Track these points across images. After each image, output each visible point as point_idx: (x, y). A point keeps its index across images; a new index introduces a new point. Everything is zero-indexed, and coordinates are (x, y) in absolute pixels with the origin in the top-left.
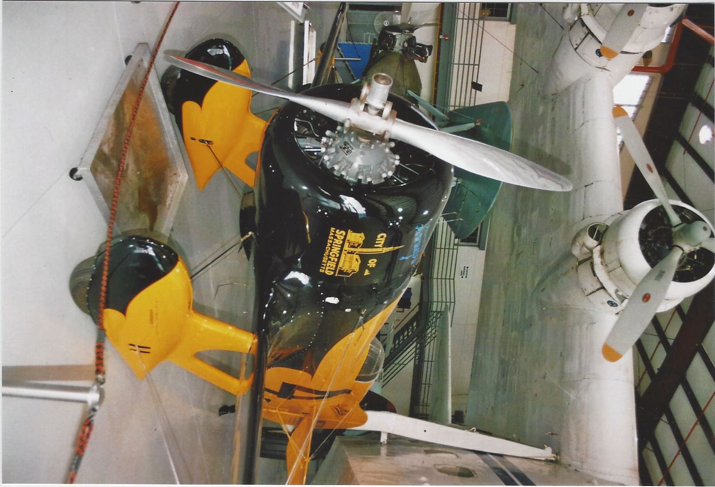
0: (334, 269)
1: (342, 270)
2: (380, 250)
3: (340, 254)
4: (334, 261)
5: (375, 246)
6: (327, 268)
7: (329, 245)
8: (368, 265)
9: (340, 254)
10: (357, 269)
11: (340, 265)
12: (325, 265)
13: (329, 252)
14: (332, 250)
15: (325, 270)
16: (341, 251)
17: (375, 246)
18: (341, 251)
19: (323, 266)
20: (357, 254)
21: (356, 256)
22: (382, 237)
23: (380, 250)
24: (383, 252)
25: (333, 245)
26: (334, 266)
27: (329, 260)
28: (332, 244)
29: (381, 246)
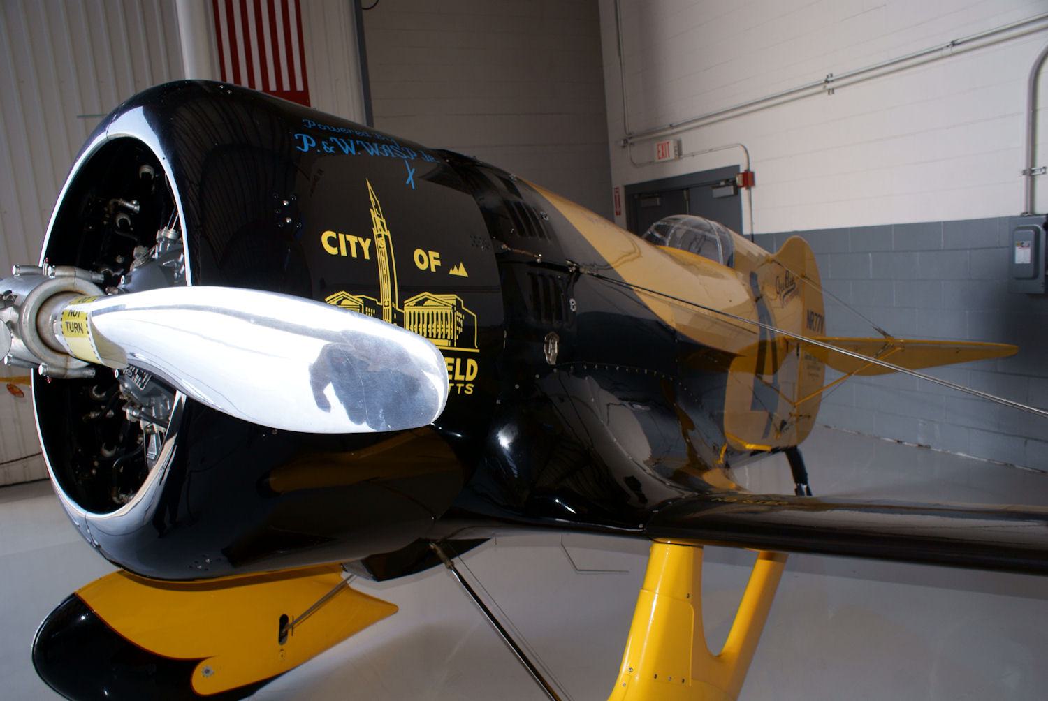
0: (459, 361)
1: (456, 337)
2: (381, 242)
5: (367, 256)
8: (433, 269)
10: (451, 299)
15: (465, 382)
17: (367, 256)
20: (401, 306)
22: (334, 242)
23: (381, 242)
24: (388, 233)
29: (368, 241)
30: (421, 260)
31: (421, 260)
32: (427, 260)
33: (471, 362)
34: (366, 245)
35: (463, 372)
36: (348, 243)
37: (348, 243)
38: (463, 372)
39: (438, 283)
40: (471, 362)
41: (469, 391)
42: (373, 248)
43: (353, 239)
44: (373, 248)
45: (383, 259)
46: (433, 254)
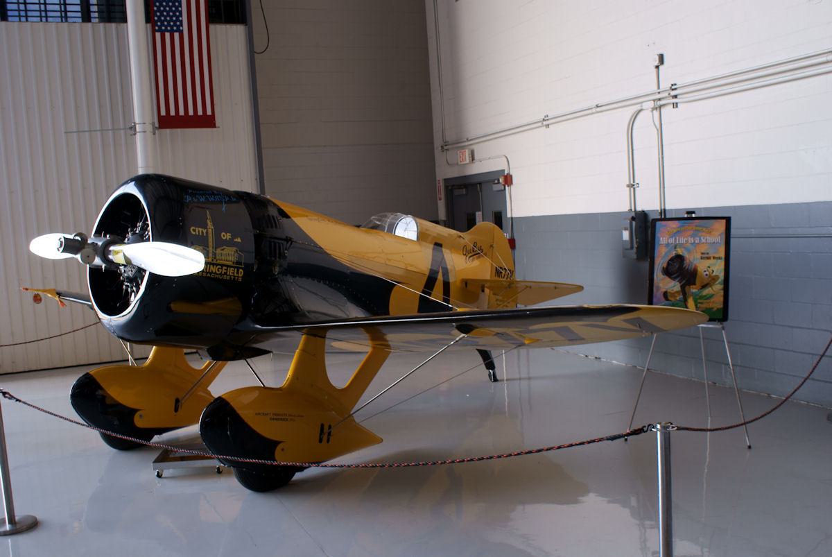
3: (217, 265)
4: (227, 270)
5: (205, 235)
6: (236, 274)
7: (209, 275)
9: (217, 265)
10: (234, 249)
11: (230, 264)
12: (232, 277)
13: (215, 273)
14: (214, 271)
16: (213, 264)
17: (205, 235)
18: (213, 264)
19: (234, 279)
21: (219, 251)
22: (194, 230)
25: (208, 271)
26: (232, 269)
27: (226, 273)
28: (207, 273)
30: (224, 236)
31: (224, 236)
32: (226, 236)
33: (241, 270)
34: (205, 231)
35: (238, 273)
36: (199, 231)
37: (199, 231)
38: (238, 273)
39: (230, 243)
40: (241, 270)
41: (240, 280)
42: (207, 233)
43: (200, 230)
44: (207, 233)
45: (210, 235)
46: (228, 234)
